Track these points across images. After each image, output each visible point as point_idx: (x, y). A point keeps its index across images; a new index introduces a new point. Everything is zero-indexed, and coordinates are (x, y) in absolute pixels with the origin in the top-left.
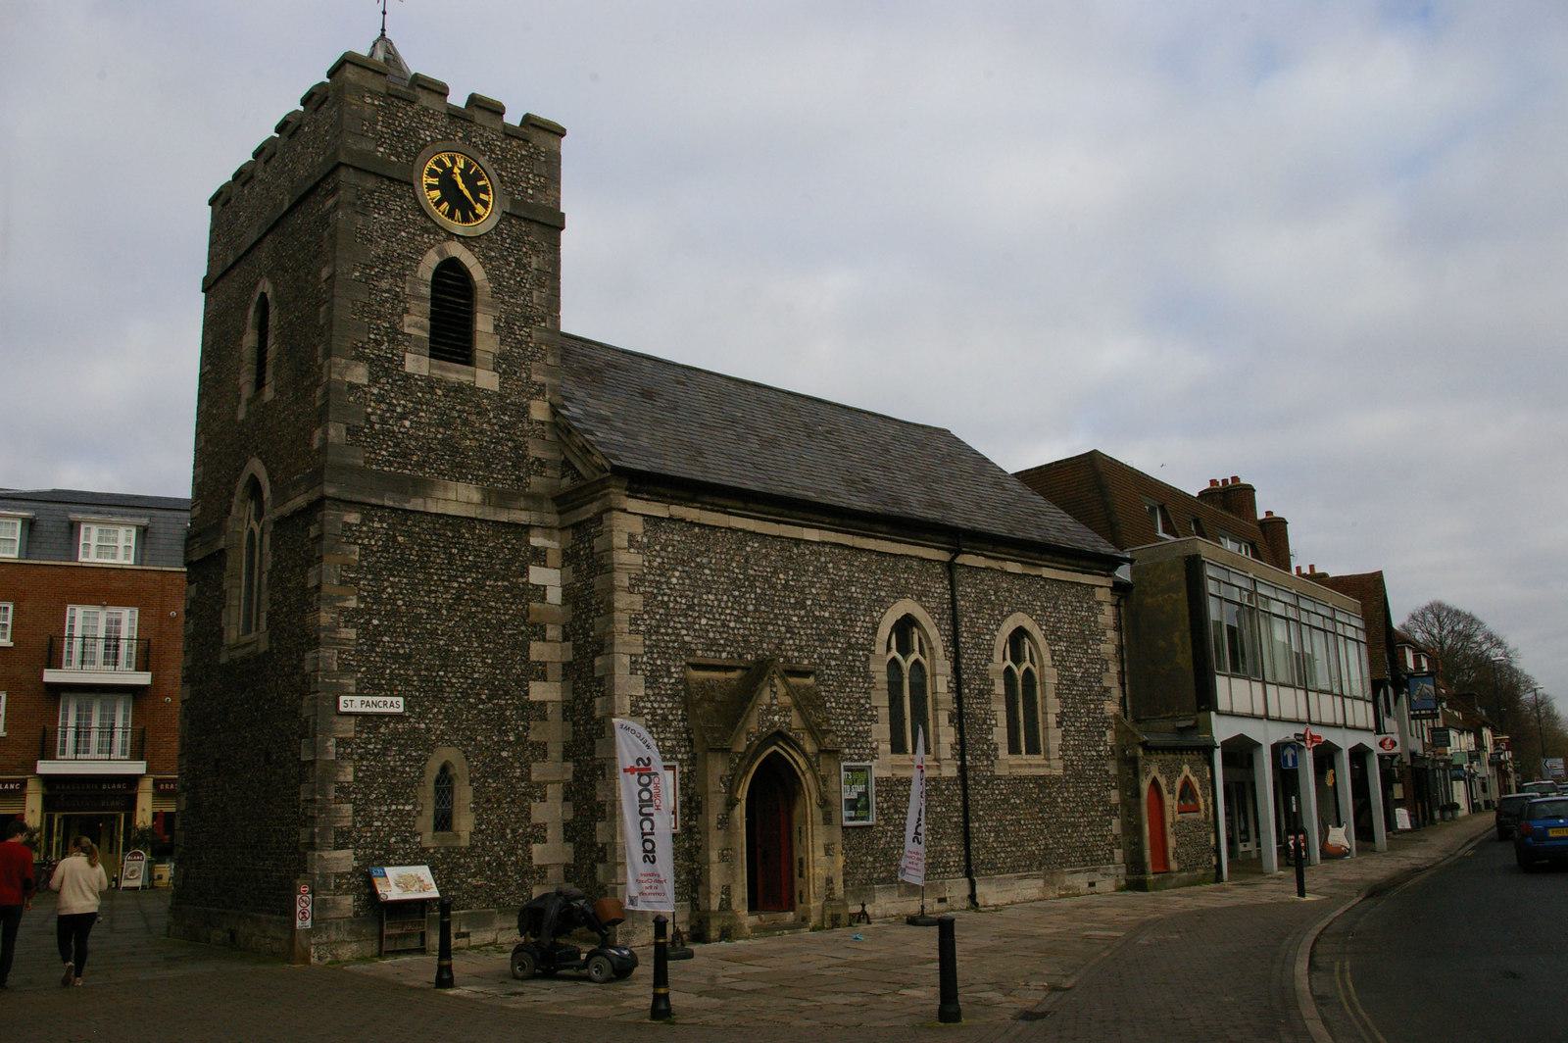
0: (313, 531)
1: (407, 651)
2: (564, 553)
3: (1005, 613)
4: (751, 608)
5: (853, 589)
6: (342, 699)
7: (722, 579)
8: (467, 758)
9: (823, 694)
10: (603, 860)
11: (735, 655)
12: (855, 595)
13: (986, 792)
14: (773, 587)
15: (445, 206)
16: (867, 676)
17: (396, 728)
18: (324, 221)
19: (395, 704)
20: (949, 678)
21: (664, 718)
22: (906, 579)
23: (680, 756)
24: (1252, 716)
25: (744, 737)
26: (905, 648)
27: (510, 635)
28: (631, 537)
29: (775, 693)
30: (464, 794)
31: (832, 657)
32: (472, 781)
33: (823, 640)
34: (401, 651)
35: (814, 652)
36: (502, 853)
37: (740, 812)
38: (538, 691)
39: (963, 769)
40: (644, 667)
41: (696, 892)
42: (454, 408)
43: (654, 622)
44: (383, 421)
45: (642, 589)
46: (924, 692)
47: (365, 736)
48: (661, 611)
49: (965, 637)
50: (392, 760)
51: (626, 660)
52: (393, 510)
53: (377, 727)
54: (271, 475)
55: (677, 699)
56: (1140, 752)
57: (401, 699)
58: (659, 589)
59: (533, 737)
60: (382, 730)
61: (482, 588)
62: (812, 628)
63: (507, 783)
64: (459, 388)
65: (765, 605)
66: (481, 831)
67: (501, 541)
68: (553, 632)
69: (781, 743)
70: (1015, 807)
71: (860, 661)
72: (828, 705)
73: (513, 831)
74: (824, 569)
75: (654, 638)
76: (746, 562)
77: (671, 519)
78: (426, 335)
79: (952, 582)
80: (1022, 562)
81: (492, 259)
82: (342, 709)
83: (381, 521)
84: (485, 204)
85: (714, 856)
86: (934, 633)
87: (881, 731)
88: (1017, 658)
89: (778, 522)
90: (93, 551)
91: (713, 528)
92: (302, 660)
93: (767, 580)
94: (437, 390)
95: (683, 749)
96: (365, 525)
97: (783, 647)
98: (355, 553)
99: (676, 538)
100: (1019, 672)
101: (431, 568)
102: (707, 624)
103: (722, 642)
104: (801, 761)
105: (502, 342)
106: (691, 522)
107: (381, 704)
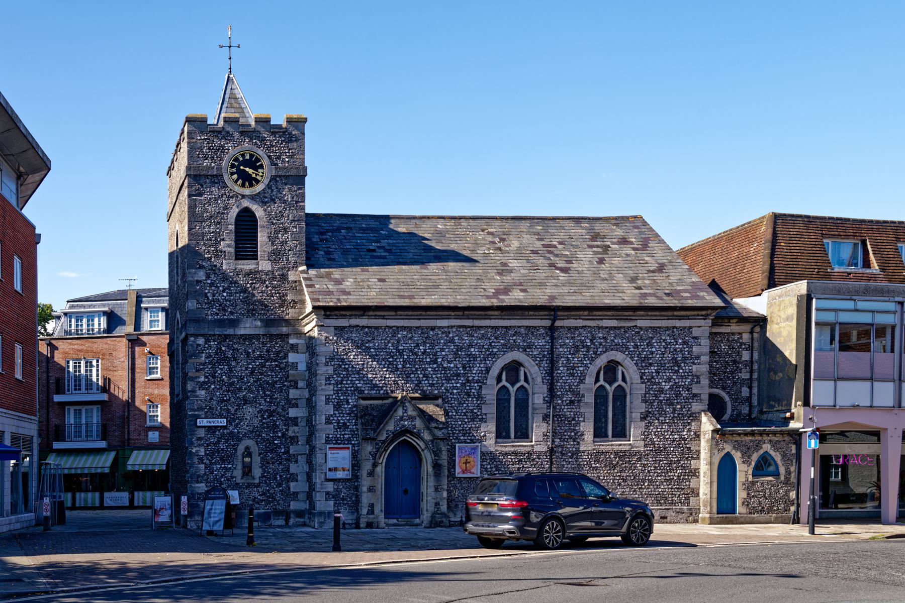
3: (598, 353)
4: (400, 366)
5: (473, 350)
6: (198, 420)
7: (382, 353)
12: (473, 353)
14: (416, 354)
15: (240, 182)
16: (479, 397)
19: (223, 422)
20: (545, 395)
21: (344, 424)
23: (353, 442)
25: (385, 433)
29: (406, 410)
31: (454, 388)
32: (260, 454)
33: (448, 380)
34: (225, 398)
35: (442, 386)
37: (380, 470)
38: (293, 413)
40: (333, 400)
42: (248, 283)
43: (339, 379)
44: (214, 295)
45: (332, 363)
46: (528, 403)
47: (209, 436)
48: (344, 373)
51: (323, 398)
52: (219, 335)
55: (352, 415)
57: (225, 420)
58: (343, 362)
60: (217, 433)
61: (264, 366)
62: (441, 374)
63: (277, 455)
65: (410, 364)
68: (301, 384)
69: (408, 435)
71: (475, 389)
72: (450, 414)
74: (452, 341)
75: (339, 386)
78: (232, 250)
79: (552, 338)
82: (198, 424)
83: (214, 341)
85: (365, 489)
91: (377, 328)
93: (411, 351)
95: (355, 439)
97: (421, 385)
99: (354, 335)
105: (273, 245)
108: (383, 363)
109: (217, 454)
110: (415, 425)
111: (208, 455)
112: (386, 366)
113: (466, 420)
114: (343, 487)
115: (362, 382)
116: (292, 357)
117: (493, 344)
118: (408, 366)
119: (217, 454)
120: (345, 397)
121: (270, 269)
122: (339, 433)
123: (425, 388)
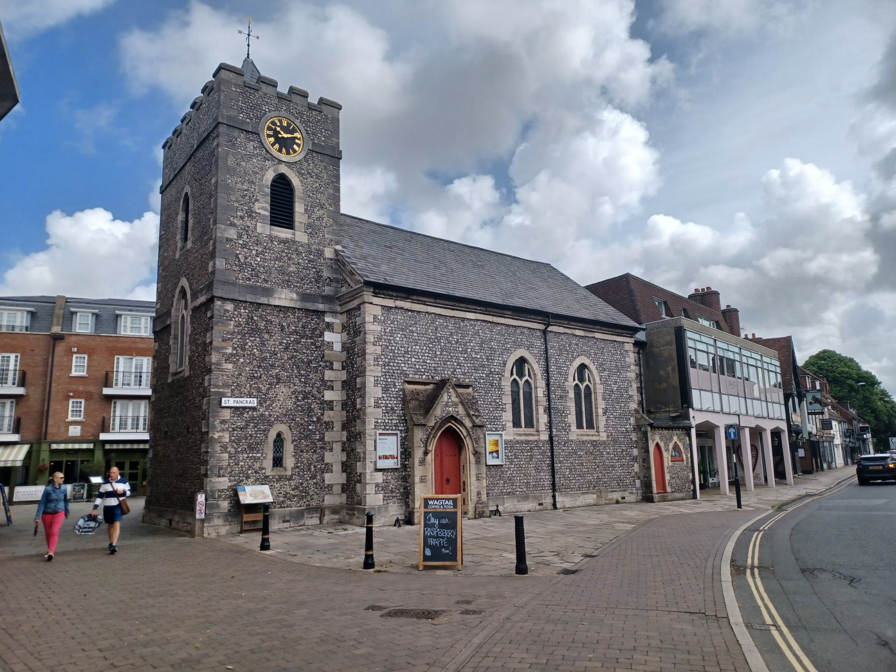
0: (209, 314)
1: (259, 375)
2: (343, 325)
4: (438, 353)
5: (493, 343)
6: (223, 399)
8: (291, 429)
9: (477, 397)
10: (359, 481)
11: (430, 377)
12: (494, 347)
13: (564, 448)
14: (450, 342)
15: (277, 146)
16: (500, 388)
17: (253, 414)
18: (212, 154)
19: (253, 402)
22: (521, 339)
23: (400, 428)
24: (714, 412)
25: (433, 418)
26: (521, 374)
27: (314, 367)
28: (375, 317)
30: (289, 448)
32: (293, 441)
33: (476, 370)
34: (256, 375)
36: (309, 478)
37: (430, 457)
38: (328, 395)
39: (551, 437)
40: (381, 383)
41: (408, 498)
43: (387, 360)
44: (246, 258)
45: (380, 343)
46: (531, 396)
47: (235, 418)
48: (391, 354)
49: (552, 368)
50: (250, 431)
51: (372, 379)
52: (251, 303)
53: (242, 414)
54: (191, 287)
55: (399, 399)
56: (649, 429)
58: (390, 343)
59: (326, 418)
60: (245, 415)
61: (299, 343)
62: (471, 363)
63: (312, 442)
64: (285, 242)
66: (298, 467)
67: (309, 319)
68: (337, 365)
69: (453, 422)
70: (580, 456)
71: (496, 380)
72: (479, 402)
73: (315, 467)
74: (477, 333)
76: (436, 330)
77: (396, 307)
78: (268, 214)
80: (584, 330)
81: (303, 174)
82: (223, 404)
83: (245, 309)
84: (299, 145)
85: (417, 479)
86: (536, 367)
87: (508, 416)
88: (581, 380)
89: (453, 309)
90: (129, 329)
92: (203, 380)
94: (274, 242)
95: (402, 425)
96: (236, 311)
97: (455, 373)
98: (232, 324)
99: (399, 317)
100: (582, 387)
101: (272, 333)
102: (415, 361)
103: (423, 370)
104: (464, 431)
106: (407, 309)
107: (245, 402)
108: (425, 348)
109: (244, 441)
110: (457, 412)
111: (233, 441)
112: (427, 351)
113: (491, 409)
114: (392, 478)
115: (407, 366)
116: (328, 336)
117: (507, 340)
118: (445, 353)
119: (244, 441)
120: (392, 380)
121: (306, 242)
122: (388, 418)
123: (459, 376)
